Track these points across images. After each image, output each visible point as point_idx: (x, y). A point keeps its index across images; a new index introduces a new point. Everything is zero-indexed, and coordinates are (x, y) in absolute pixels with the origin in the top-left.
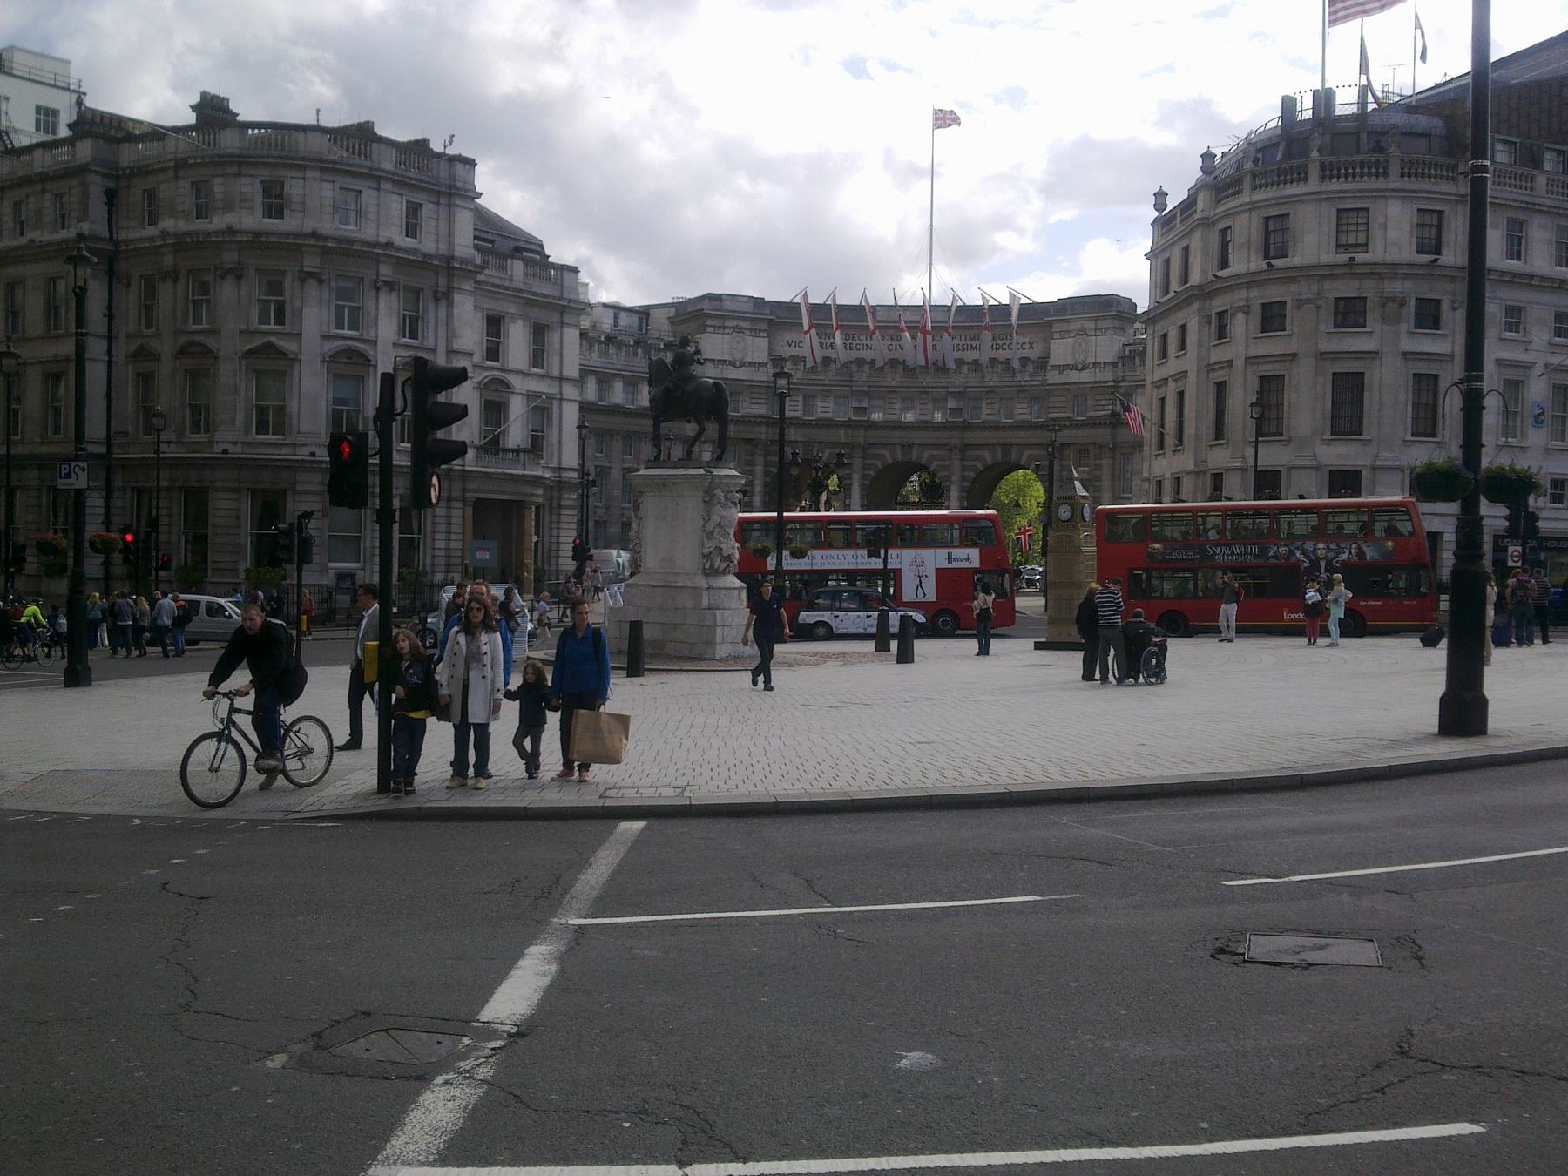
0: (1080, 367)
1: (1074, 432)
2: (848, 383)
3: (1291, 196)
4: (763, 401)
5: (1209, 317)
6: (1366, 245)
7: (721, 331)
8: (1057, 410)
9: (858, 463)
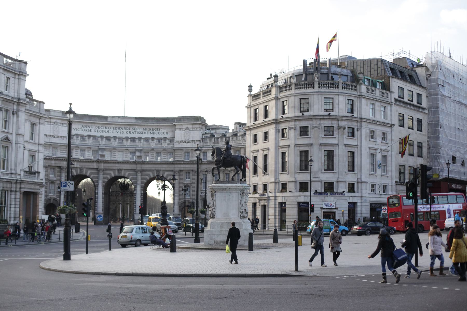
0: (187, 142)
1: (184, 166)
2: (98, 145)
3: (309, 92)
4: (65, 152)
5: (279, 130)
6: (333, 109)
7: (50, 123)
8: (178, 157)
9: (101, 176)
